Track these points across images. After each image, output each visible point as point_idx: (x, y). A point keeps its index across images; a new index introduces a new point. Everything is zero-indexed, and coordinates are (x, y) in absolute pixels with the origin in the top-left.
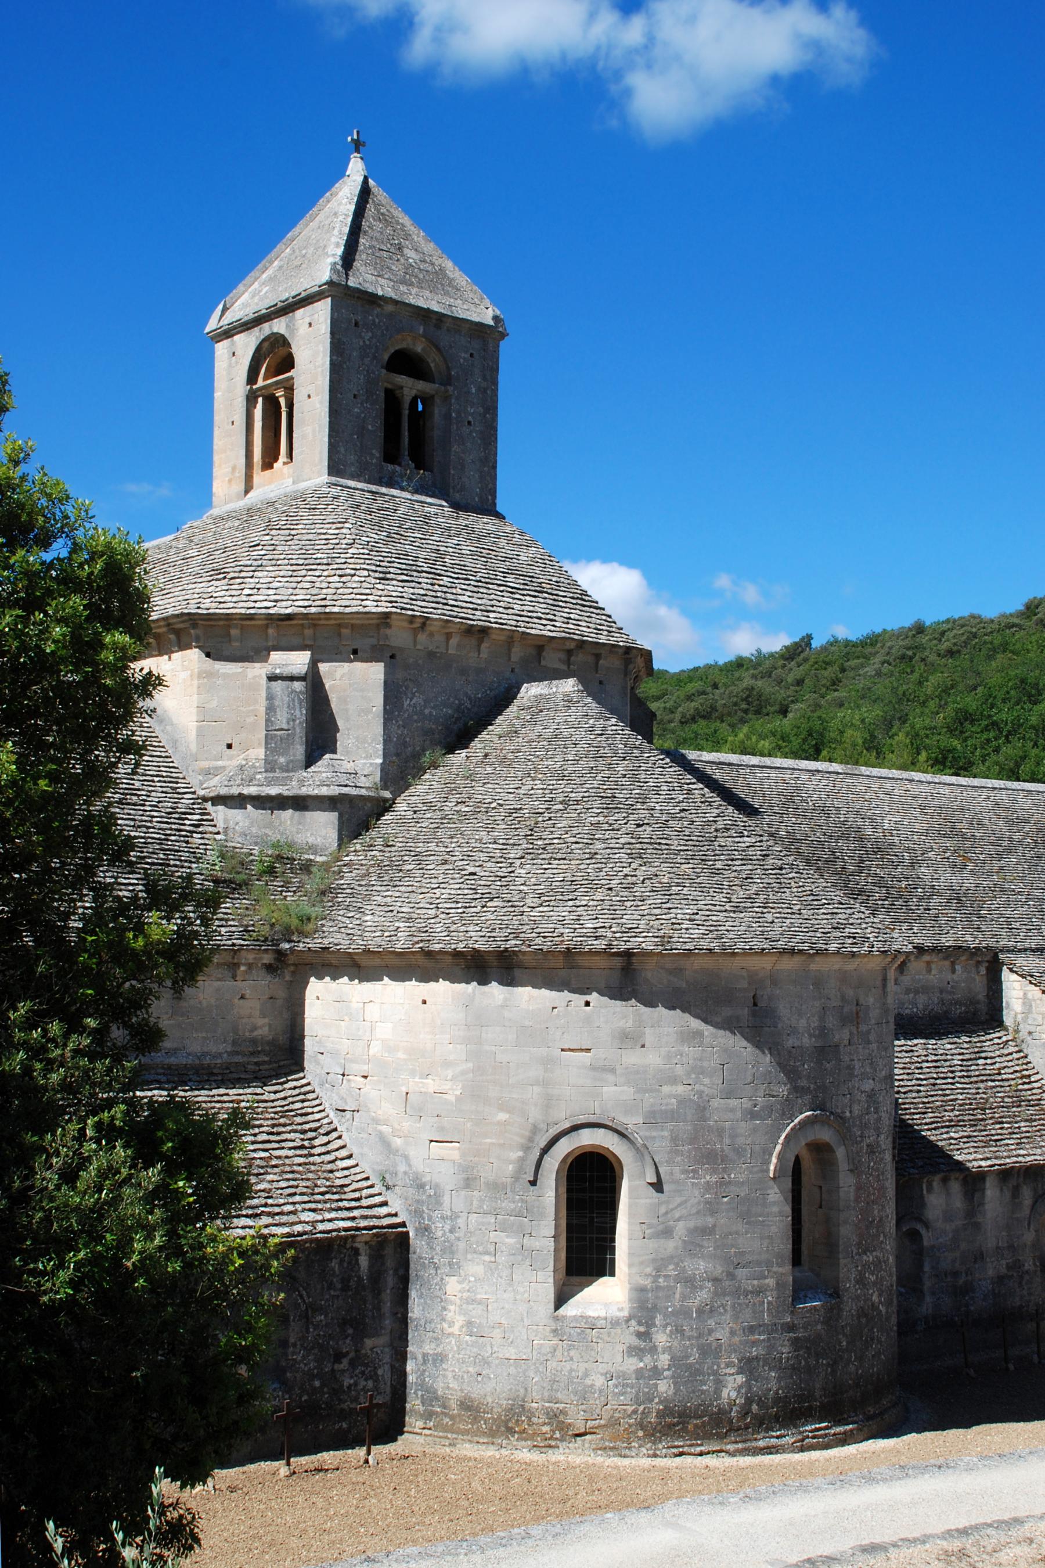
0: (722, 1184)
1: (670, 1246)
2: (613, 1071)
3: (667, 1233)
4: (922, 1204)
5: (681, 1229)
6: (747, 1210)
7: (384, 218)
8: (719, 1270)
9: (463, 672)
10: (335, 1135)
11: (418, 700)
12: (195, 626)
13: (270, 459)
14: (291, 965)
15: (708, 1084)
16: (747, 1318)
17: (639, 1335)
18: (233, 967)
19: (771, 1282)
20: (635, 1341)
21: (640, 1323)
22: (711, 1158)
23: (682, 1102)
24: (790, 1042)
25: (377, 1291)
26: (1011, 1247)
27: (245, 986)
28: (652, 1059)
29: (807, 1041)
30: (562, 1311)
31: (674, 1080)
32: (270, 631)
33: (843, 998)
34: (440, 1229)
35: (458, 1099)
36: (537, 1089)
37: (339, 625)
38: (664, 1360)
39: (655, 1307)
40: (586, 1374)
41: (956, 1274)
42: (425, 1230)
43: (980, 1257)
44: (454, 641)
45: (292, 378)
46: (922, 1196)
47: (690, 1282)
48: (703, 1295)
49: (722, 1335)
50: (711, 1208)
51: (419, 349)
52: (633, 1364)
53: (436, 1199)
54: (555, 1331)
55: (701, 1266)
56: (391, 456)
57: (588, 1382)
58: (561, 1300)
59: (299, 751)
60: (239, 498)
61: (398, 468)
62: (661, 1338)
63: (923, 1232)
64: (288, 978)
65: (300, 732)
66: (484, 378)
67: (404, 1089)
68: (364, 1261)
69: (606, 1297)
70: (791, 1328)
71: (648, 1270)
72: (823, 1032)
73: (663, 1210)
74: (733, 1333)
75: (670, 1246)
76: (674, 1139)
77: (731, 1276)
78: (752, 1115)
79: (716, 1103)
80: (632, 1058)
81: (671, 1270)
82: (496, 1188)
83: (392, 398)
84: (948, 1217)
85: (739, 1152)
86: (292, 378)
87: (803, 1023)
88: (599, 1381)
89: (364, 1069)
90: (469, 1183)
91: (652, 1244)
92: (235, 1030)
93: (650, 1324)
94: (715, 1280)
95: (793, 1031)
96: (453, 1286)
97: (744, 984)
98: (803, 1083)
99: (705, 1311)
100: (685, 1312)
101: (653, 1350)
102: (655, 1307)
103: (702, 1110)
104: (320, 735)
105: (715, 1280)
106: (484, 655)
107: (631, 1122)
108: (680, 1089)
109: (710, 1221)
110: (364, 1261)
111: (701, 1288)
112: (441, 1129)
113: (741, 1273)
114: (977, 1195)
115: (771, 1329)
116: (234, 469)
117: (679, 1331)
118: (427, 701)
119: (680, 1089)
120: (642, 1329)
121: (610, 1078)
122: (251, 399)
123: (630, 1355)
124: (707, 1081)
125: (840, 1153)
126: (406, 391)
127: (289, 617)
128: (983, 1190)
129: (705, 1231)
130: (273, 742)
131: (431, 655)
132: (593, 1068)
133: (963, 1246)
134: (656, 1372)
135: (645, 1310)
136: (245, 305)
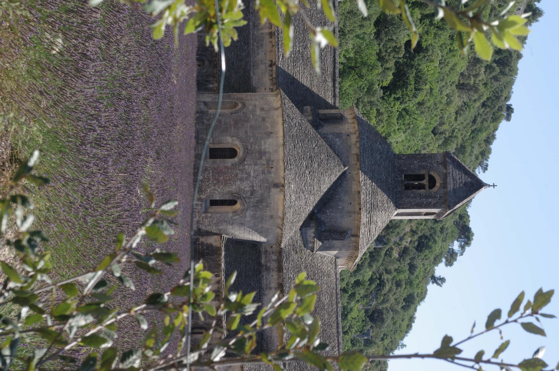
11: (339, 143)
24: (263, 142)
29: (263, 147)
33: (273, 161)
51: (437, 184)
61: (403, 178)
66: (434, 204)
68: (211, 86)
72: (265, 153)
78: (246, 133)
79: (249, 125)
83: (421, 177)
87: (267, 146)
92: (258, 88)
95: (265, 144)
98: (253, 146)
107: (244, 110)
118: (339, 146)
125: (236, 159)
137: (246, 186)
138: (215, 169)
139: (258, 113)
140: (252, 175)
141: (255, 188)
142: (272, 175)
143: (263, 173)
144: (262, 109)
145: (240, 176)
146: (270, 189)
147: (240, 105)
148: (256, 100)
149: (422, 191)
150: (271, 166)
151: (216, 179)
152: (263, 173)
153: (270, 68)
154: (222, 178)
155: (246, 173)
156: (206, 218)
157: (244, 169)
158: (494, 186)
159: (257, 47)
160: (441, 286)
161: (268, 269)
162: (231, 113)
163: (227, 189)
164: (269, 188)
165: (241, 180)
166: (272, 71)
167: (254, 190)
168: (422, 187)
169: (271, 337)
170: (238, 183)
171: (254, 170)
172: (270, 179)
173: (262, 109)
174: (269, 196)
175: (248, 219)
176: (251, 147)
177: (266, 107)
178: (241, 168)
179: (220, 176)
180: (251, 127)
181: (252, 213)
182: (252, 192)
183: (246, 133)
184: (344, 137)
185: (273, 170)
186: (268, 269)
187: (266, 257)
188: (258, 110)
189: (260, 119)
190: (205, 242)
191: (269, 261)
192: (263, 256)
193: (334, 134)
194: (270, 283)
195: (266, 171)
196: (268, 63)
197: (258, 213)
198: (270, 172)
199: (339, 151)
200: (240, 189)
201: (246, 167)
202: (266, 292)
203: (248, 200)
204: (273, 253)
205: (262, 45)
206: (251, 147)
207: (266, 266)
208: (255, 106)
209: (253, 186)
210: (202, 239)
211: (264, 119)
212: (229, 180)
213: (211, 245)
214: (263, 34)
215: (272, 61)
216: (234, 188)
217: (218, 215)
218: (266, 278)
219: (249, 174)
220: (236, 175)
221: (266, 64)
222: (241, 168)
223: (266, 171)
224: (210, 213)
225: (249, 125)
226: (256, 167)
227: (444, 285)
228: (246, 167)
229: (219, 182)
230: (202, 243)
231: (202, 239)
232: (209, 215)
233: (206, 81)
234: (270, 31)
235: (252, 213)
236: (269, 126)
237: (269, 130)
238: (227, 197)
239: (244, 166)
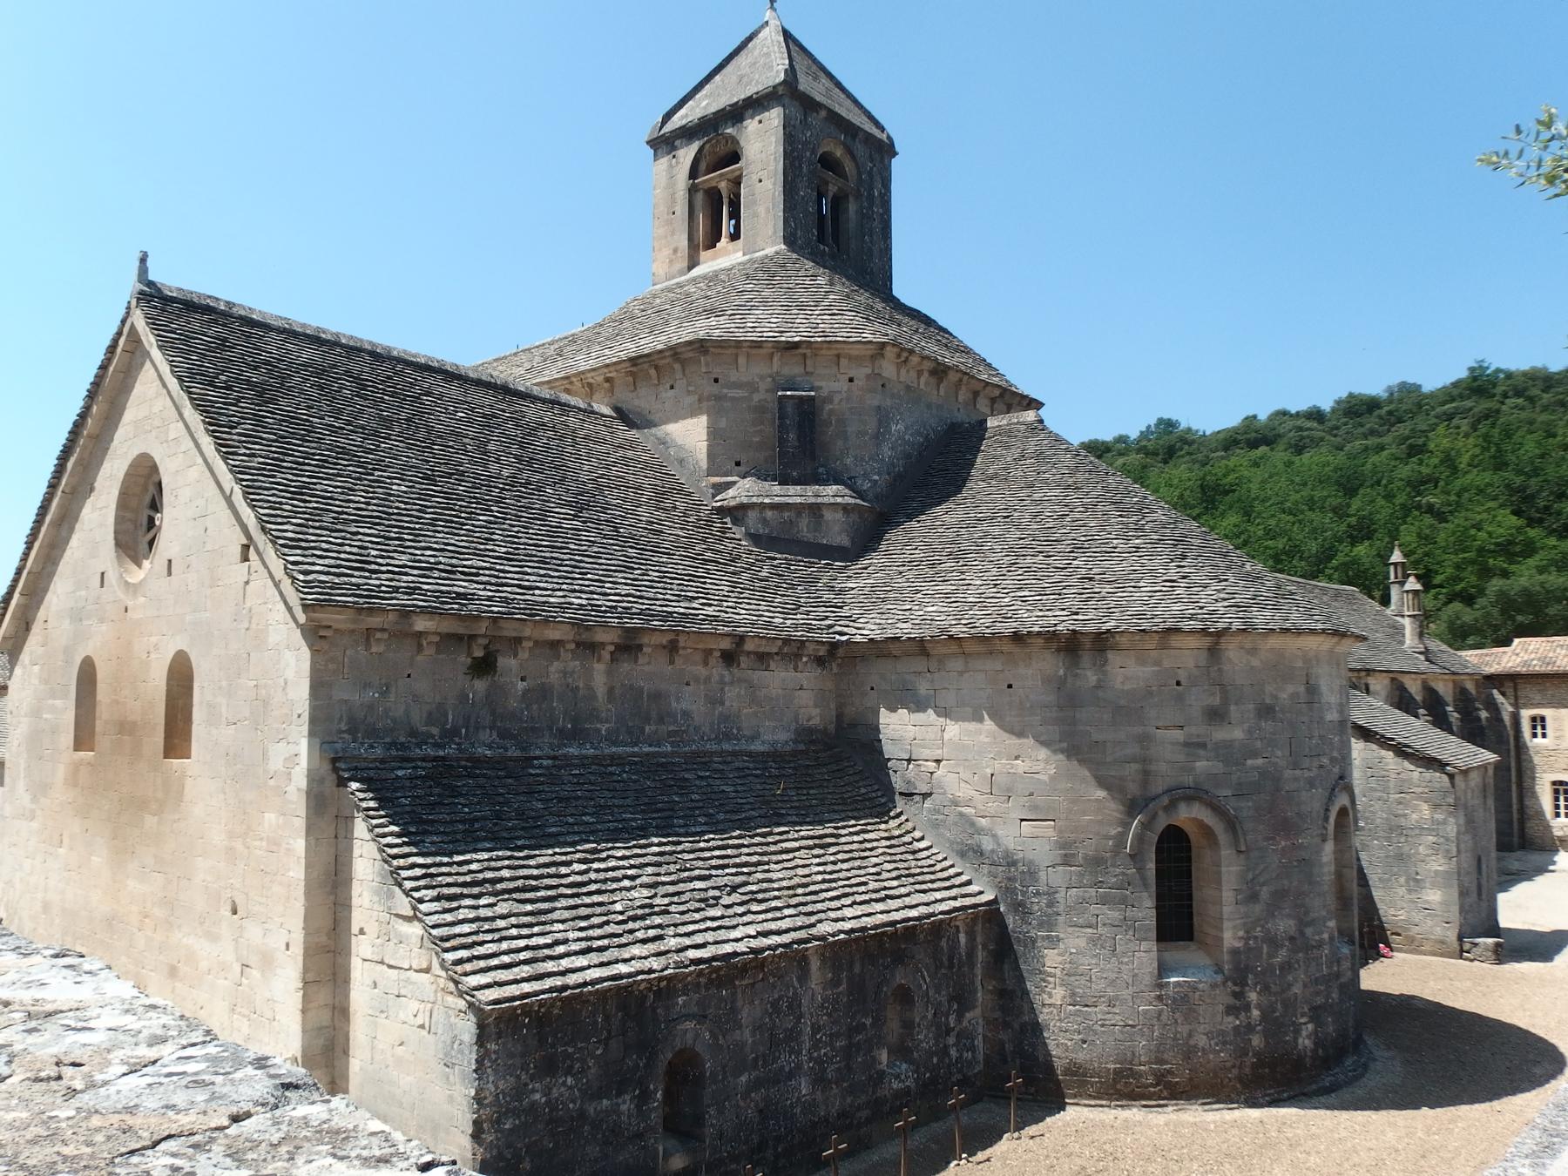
1: (1258, 909)
2: (1203, 746)
3: (1253, 897)
5: (1265, 893)
9: (929, 406)
10: (903, 818)
12: (706, 352)
13: (713, 239)
17: (1236, 995)
18: (798, 656)
19: (1326, 936)
20: (1231, 1001)
21: (1235, 984)
23: (1263, 773)
25: (972, 965)
32: (775, 359)
34: (1038, 905)
35: (1052, 778)
36: (1134, 766)
37: (838, 356)
38: (1256, 1013)
39: (1247, 967)
40: (1190, 1035)
42: (1020, 907)
44: (923, 380)
45: (741, 169)
47: (1274, 942)
48: (1282, 956)
52: (1232, 1022)
53: (1032, 874)
54: (1160, 998)
56: (821, 239)
57: (1192, 1042)
60: (682, 274)
62: (1253, 996)
64: (835, 670)
67: (989, 771)
68: (962, 938)
71: (1241, 933)
73: (1250, 876)
74: (1305, 986)
77: (1302, 933)
79: (1288, 773)
86: (741, 169)
88: (1202, 1041)
89: (938, 754)
90: (1067, 861)
91: (1242, 909)
93: (1242, 983)
96: (1052, 959)
97: (1300, 664)
99: (1287, 967)
102: (1247, 967)
105: (1292, 939)
106: (942, 392)
108: (1260, 761)
110: (962, 938)
111: (1282, 946)
112: (1035, 808)
116: (675, 251)
117: (1266, 989)
120: (1237, 989)
121: (1202, 752)
122: (692, 190)
123: (1228, 1014)
124: (1279, 753)
126: (831, 187)
127: (796, 345)
131: (908, 387)
132: (1186, 744)
134: (1250, 1028)
136: (682, 117)
139: (1238, 734)
144: (1216, 715)
159: (661, 720)
173: (1216, 715)
177: (1200, 699)
180: (1296, 766)
184: (889, 402)
188: (1220, 734)
189: (1268, 726)
196: (717, 670)
205: (657, 696)
208: (1193, 746)
211: (1266, 711)
214: (611, 691)
225: (1288, 773)
233: (951, 966)
236: (1290, 689)
237: (1302, 689)
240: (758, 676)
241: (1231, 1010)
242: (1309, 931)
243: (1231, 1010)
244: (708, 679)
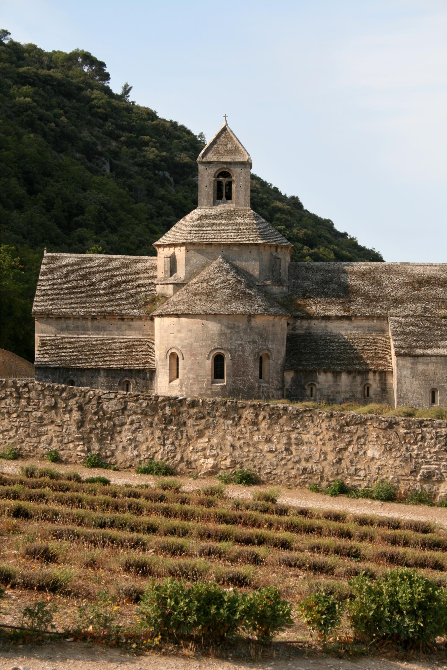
0: (195, 359)
1: (185, 371)
3: (185, 369)
4: (316, 377)
5: (187, 368)
6: (200, 365)
7: (226, 137)
8: (194, 376)
11: (195, 261)
14: (152, 319)
15: (192, 340)
16: (200, 386)
19: (206, 379)
22: (193, 355)
23: (188, 344)
24: (211, 332)
26: (352, 391)
27: (146, 323)
28: (182, 335)
29: (216, 332)
30: (171, 384)
31: (186, 339)
33: (228, 324)
38: (184, 392)
41: (329, 396)
43: (339, 392)
46: (316, 376)
47: (189, 378)
48: (191, 381)
49: (195, 389)
50: (193, 364)
55: (191, 375)
58: (170, 381)
59: (169, 273)
62: (184, 389)
63: (316, 384)
65: (169, 269)
69: (176, 382)
70: (211, 389)
75: (185, 371)
76: (186, 351)
77: (197, 378)
78: (202, 346)
79: (194, 344)
80: (180, 335)
81: (186, 376)
82: (162, 360)
84: (326, 381)
85: (199, 354)
90: (160, 359)
93: (182, 386)
94: (194, 378)
99: (192, 384)
100: (188, 384)
101: (182, 391)
103: (191, 345)
104: (173, 270)
105: (194, 378)
107: (179, 347)
108: (187, 341)
109: (193, 367)
113: (199, 378)
114: (338, 377)
115: (206, 389)
117: (187, 388)
118: (197, 261)
119: (187, 341)
128: (341, 376)
129: (192, 369)
130: (165, 272)
133: (332, 389)
135: (181, 384)
137: (249, 348)
138: (234, 375)
140: (240, 342)
141: (251, 340)
142: (241, 324)
143: (238, 332)
144: (179, 331)
145: (241, 353)
146: (252, 327)
147: (173, 350)
148: (168, 336)
149: (234, 186)
150: (233, 326)
151: (243, 374)
152: (238, 332)
153: (125, 320)
154: (242, 369)
155: (238, 348)
156: (273, 383)
157: (235, 349)
158: (225, 117)
160: (131, 88)
161: (309, 328)
162: (183, 359)
163: (251, 364)
164: (251, 328)
165: (244, 352)
166: (128, 319)
167: (253, 341)
168: (229, 184)
169: (369, 327)
170: (246, 354)
171: (236, 340)
172: (243, 327)
174: (258, 328)
175: (274, 346)
176: (215, 342)
178: (234, 352)
179: (240, 371)
181: (270, 343)
182: (254, 342)
183: (202, 346)
185: (236, 324)
186: (309, 328)
187: (298, 329)
190: (290, 383)
191: (302, 327)
192: (297, 332)
193: (186, 265)
194: (321, 327)
195: (237, 330)
197: (271, 337)
198: (238, 327)
199: (202, 261)
200: (252, 353)
201: (233, 347)
202: (329, 330)
203: (260, 346)
204: (295, 323)
206: (215, 342)
207: (306, 329)
208: (175, 337)
209: (249, 342)
210: (287, 386)
212: (244, 362)
213: (292, 378)
214: (92, 326)
215: (119, 319)
216: (251, 359)
217: (271, 372)
218: (317, 330)
219: (240, 345)
220: (240, 356)
221: (121, 324)
222: (234, 352)
223: (237, 330)
224: (269, 379)
226: (234, 338)
227: (130, 85)
228: (233, 347)
229: (245, 371)
230: (290, 386)
231: (287, 386)
232: (271, 380)
234: (90, 319)
235: (270, 343)
238: (258, 364)
239: (232, 349)
240: (131, 323)
241: (180, 391)
242: (199, 378)
243: (180, 391)
244: (117, 324)
